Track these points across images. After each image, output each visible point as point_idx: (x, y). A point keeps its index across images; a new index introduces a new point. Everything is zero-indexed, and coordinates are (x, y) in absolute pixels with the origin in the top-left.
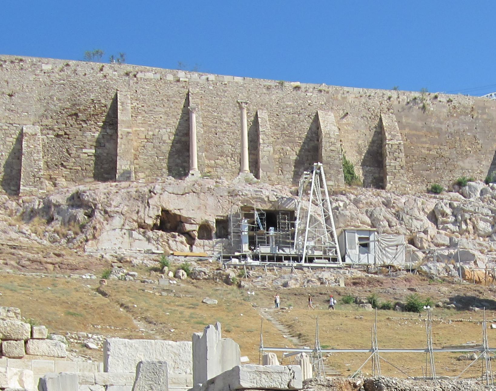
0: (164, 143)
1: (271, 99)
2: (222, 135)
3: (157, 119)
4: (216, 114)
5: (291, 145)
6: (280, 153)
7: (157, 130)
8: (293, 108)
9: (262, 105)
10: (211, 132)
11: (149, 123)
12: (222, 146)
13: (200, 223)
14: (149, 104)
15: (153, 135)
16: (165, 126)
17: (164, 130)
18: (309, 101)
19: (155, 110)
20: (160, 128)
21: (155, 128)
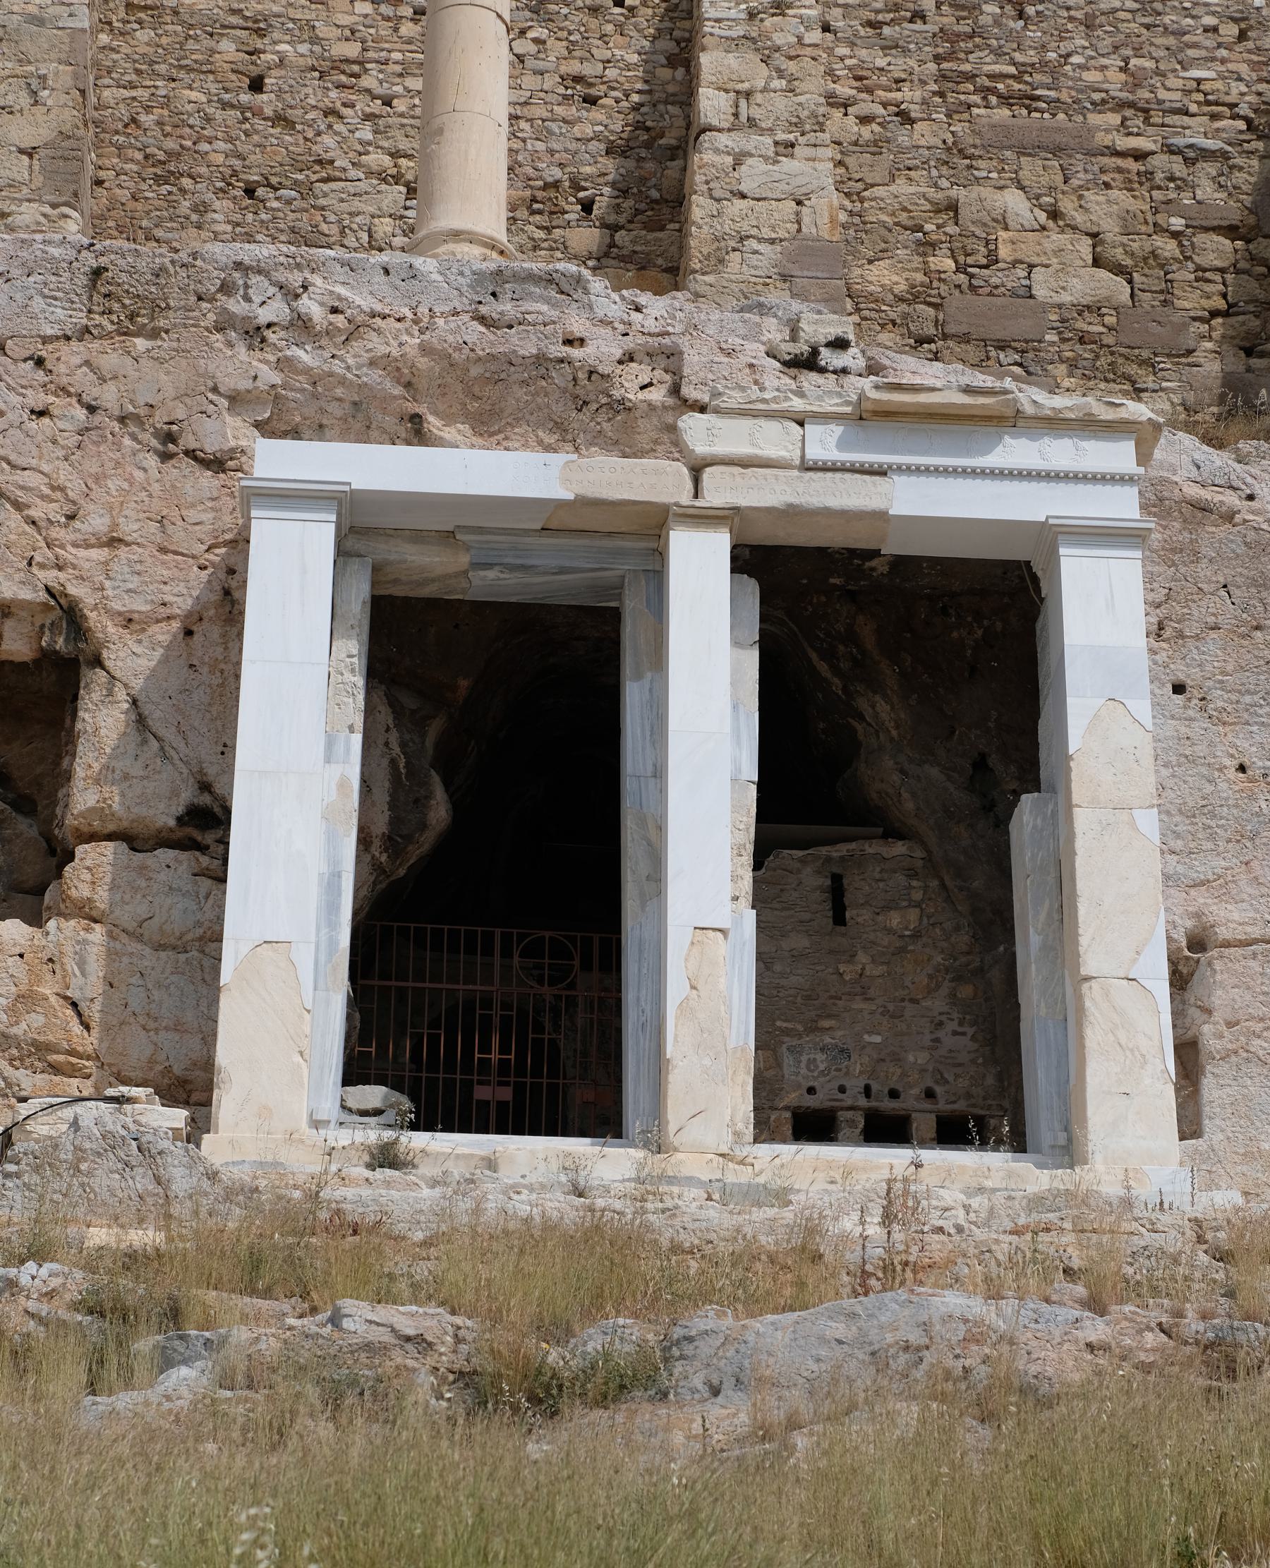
2: (314, 94)
5: (1030, 169)
10: (205, 69)
12: (306, 190)
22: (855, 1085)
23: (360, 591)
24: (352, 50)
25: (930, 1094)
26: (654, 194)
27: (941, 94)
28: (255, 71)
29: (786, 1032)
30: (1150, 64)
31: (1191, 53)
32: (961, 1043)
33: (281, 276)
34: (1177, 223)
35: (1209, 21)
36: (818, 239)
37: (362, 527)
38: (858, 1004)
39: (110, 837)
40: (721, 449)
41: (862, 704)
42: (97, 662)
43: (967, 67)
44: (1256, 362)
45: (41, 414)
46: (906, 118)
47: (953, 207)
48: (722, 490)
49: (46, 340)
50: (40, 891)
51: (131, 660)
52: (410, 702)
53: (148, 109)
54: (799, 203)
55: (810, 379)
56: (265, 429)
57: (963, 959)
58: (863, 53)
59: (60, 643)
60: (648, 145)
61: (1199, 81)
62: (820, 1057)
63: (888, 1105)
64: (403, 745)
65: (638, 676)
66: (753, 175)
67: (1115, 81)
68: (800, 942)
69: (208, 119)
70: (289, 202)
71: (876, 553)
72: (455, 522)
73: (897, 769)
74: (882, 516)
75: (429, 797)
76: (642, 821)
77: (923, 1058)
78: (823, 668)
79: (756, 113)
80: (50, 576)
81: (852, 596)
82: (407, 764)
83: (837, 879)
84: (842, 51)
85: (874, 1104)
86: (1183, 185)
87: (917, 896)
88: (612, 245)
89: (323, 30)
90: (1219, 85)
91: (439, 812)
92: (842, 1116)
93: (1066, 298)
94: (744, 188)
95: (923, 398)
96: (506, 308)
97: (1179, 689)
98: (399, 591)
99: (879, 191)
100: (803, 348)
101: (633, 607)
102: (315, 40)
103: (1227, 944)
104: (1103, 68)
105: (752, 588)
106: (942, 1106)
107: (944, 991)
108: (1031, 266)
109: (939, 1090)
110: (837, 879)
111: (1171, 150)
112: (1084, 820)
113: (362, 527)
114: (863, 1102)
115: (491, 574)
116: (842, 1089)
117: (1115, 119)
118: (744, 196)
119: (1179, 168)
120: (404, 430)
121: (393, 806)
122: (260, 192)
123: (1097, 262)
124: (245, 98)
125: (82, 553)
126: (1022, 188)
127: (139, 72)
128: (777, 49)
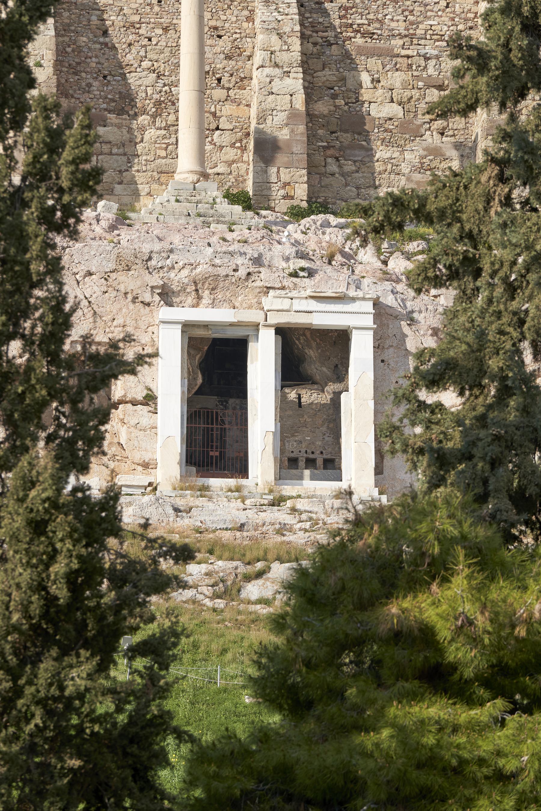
6: (334, 97)
22: (303, 450)
24: (136, 18)
25: (322, 453)
26: (243, 76)
31: (429, 14)
32: (329, 439)
34: (421, 84)
36: (298, 110)
37: (187, 327)
38: (304, 429)
41: (306, 351)
43: (350, 21)
44: (444, 139)
47: (344, 79)
48: (274, 319)
49: (106, 273)
53: (69, 46)
54: (291, 95)
58: (315, 15)
61: (431, 26)
63: (311, 456)
68: (290, 413)
69: (89, 48)
70: (119, 81)
84: (307, 15)
88: (228, 96)
91: (200, 381)
92: (300, 459)
93: (381, 115)
94: (273, 91)
97: (383, 361)
99: (319, 74)
104: (398, 21)
105: (280, 338)
106: (325, 456)
108: (370, 103)
111: (419, 55)
114: (305, 455)
117: (401, 42)
118: (273, 93)
119: (422, 63)
122: (109, 78)
124: (101, 40)
127: (65, 30)
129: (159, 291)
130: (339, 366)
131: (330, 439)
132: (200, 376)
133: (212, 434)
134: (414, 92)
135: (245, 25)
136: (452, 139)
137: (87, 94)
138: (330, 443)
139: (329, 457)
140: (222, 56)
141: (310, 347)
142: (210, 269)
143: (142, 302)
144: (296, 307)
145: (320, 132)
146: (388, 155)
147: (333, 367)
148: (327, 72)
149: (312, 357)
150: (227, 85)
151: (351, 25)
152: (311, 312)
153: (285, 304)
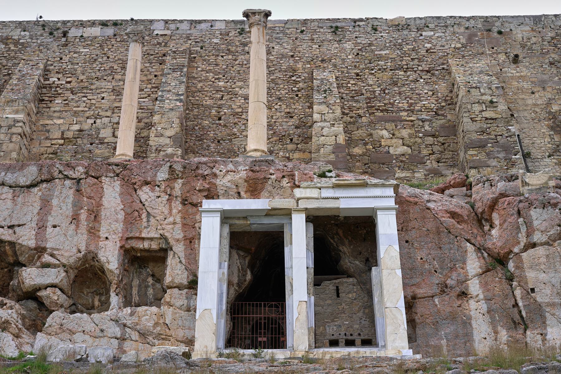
0: (101, 143)
1: (344, 49)
2: (232, 120)
3: (93, 102)
4: (221, 84)
5: (388, 125)
6: (366, 144)
7: (91, 121)
8: (393, 60)
9: (323, 61)
10: (209, 116)
11: (74, 109)
12: (230, 140)
13: (72, 260)
14: (82, 77)
15: (81, 131)
16: (109, 113)
17: (106, 120)
18: (428, 46)
19: (93, 87)
20: (98, 117)
21: (88, 118)
23: (227, 230)
24: (240, 110)
25: (359, 334)
26: (306, 136)
27: (368, 111)
28: (219, 116)
29: (327, 322)
30: (413, 101)
31: (422, 98)
32: (366, 323)
33: (209, 165)
34: (421, 135)
35: (426, 91)
36: (341, 144)
37: (226, 217)
39: (175, 287)
40: (303, 196)
41: (341, 248)
42: (171, 249)
44: (440, 164)
45: (159, 197)
46: (360, 117)
47: (371, 135)
48: (303, 205)
50: (160, 300)
51: (179, 249)
52: (242, 253)
53: (197, 126)
55: (323, 179)
56: (207, 197)
57: (366, 304)
58: (350, 103)
59: (164, 246)
60: (304, 126)
61: (424, 104)
62: (335, 327)
63: (350, 338)
64: (240, 263)
65: (287, 246)
66: (325, 131)
67: (406, 106)
69: (210, 127)
71: (339, 216)
72: (246, 214)
73: (349, 262)
74: (338, 208)
75: (246, 274)
76: (289, 278)
77: (357, 326)
78: (332, 241)
79: (326, 118)
80: (161, 232)
81: (337, 225)
82: (242, 267)
83: (337, 287)
85: (347, 337)
86: (423, 127)
87: (355, 290)
88: (297, 148)
89: (233, 106)
90: (429, 105)
91: (249, 277)
92: (340, 340)
93: (397, 153)
95: (346, 182)
96: (257, 168)
97: (407, 242)
98: (236, 230)
100: (321, 172)
101: (286, 230)
102: (232, 109)
103: (420, 298)
104: (403, 103)
105: (311, 226)
106: (362, 337)
107: (362, 311)
109: (361, 333)
110: (337, 287)
111: (418, 119)
112: (385, 273)
113: (226, 217)
114: (344, 337)
115: (255, 226)
116: (340, 334)
117: (406, 114)
118: (324, 136)
119: (421, 123)
120: (236, 195)
121: (238, 276)
122: (221, 142)
123: (403, 145)
124: (217, 122)
125: (168, 226)
126: (386, 130)
128: (330, 104)
129: (205, 194)
130: (370, 259)
131: (367, 323)
132: (249, 273)
133: (265, 329)
134: (417, 139)
135: (307, 110)
136: (445, 164)
137: (207, 151)
138: (367, 326)
139: (366, 337)
140: (293, 127)
141: (343, 244)
142: (250, 174)
143: (190, 203)
144: (323, 195)
145: (358, 164)
146: (403, 175)
147: (364, 260)
148: (360, 131)
149: (343, 244)
150: (297, 142)
151: (373, 107)
152: (338, 198)
153: (314, 193)
